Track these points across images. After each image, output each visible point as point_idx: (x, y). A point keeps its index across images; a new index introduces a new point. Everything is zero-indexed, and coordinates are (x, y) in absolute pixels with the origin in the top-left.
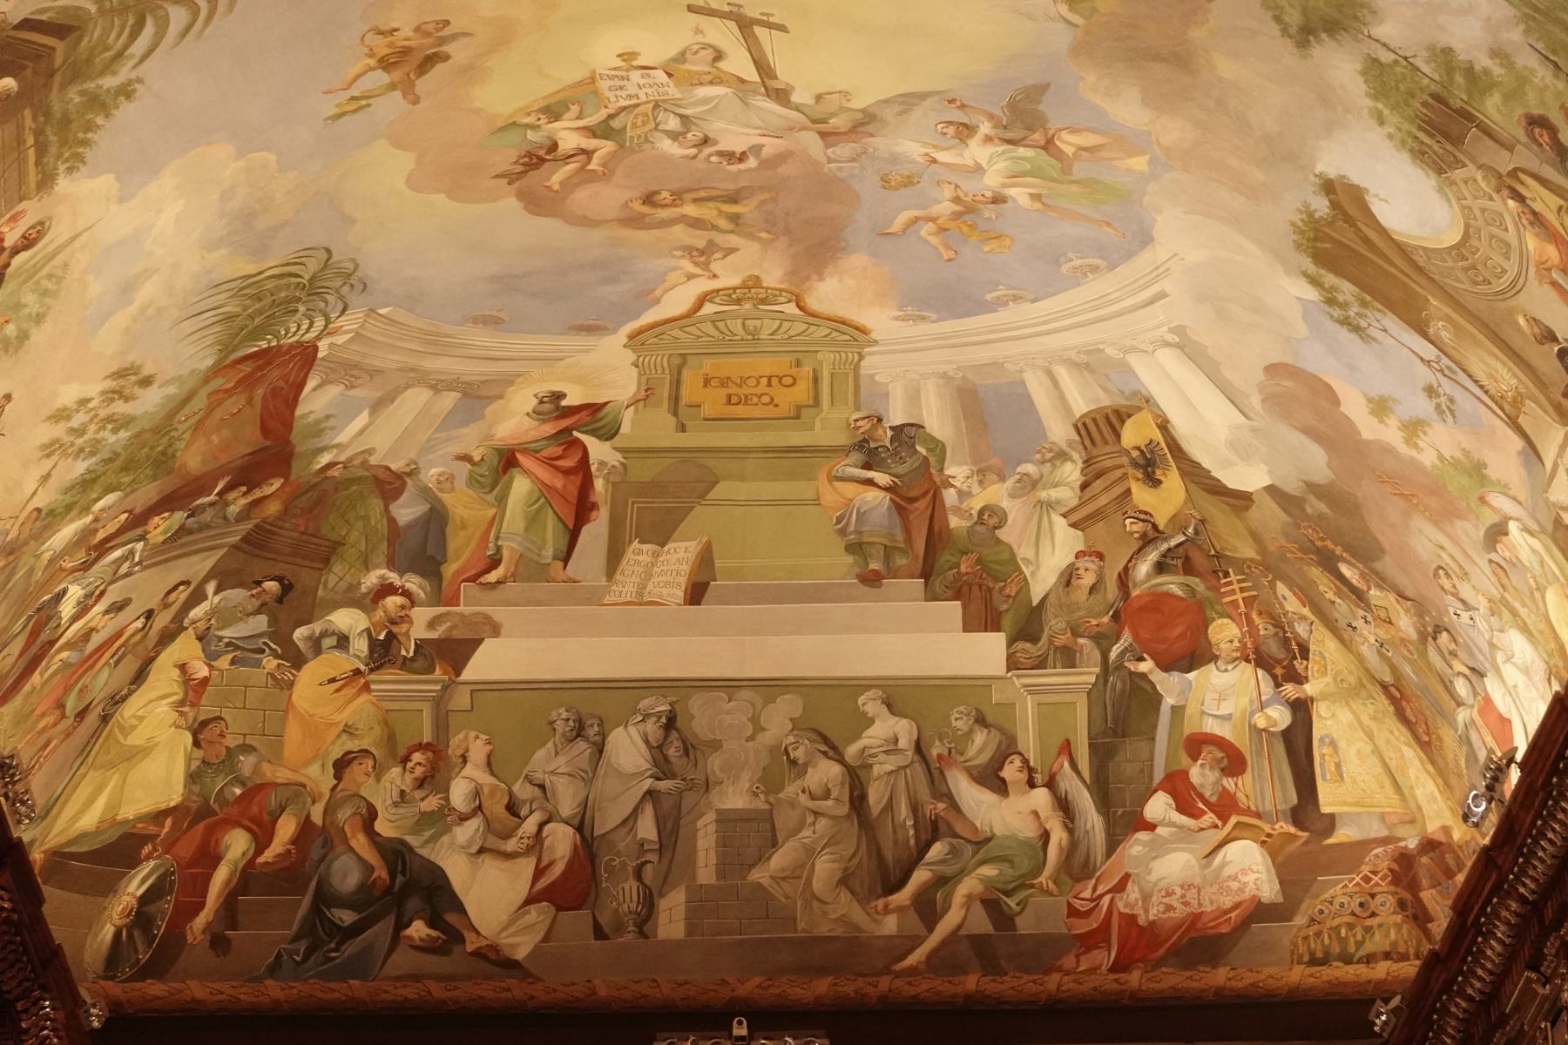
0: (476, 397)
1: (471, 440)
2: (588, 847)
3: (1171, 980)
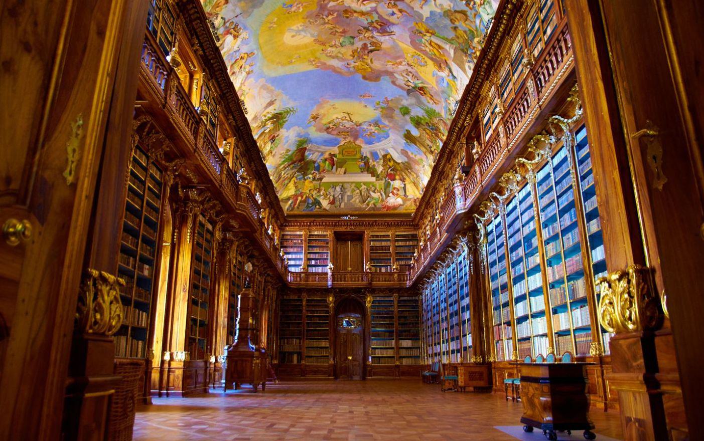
0: (323, 153)
1: (322, 158)
2: (334, 199)
3: (392, 212)
